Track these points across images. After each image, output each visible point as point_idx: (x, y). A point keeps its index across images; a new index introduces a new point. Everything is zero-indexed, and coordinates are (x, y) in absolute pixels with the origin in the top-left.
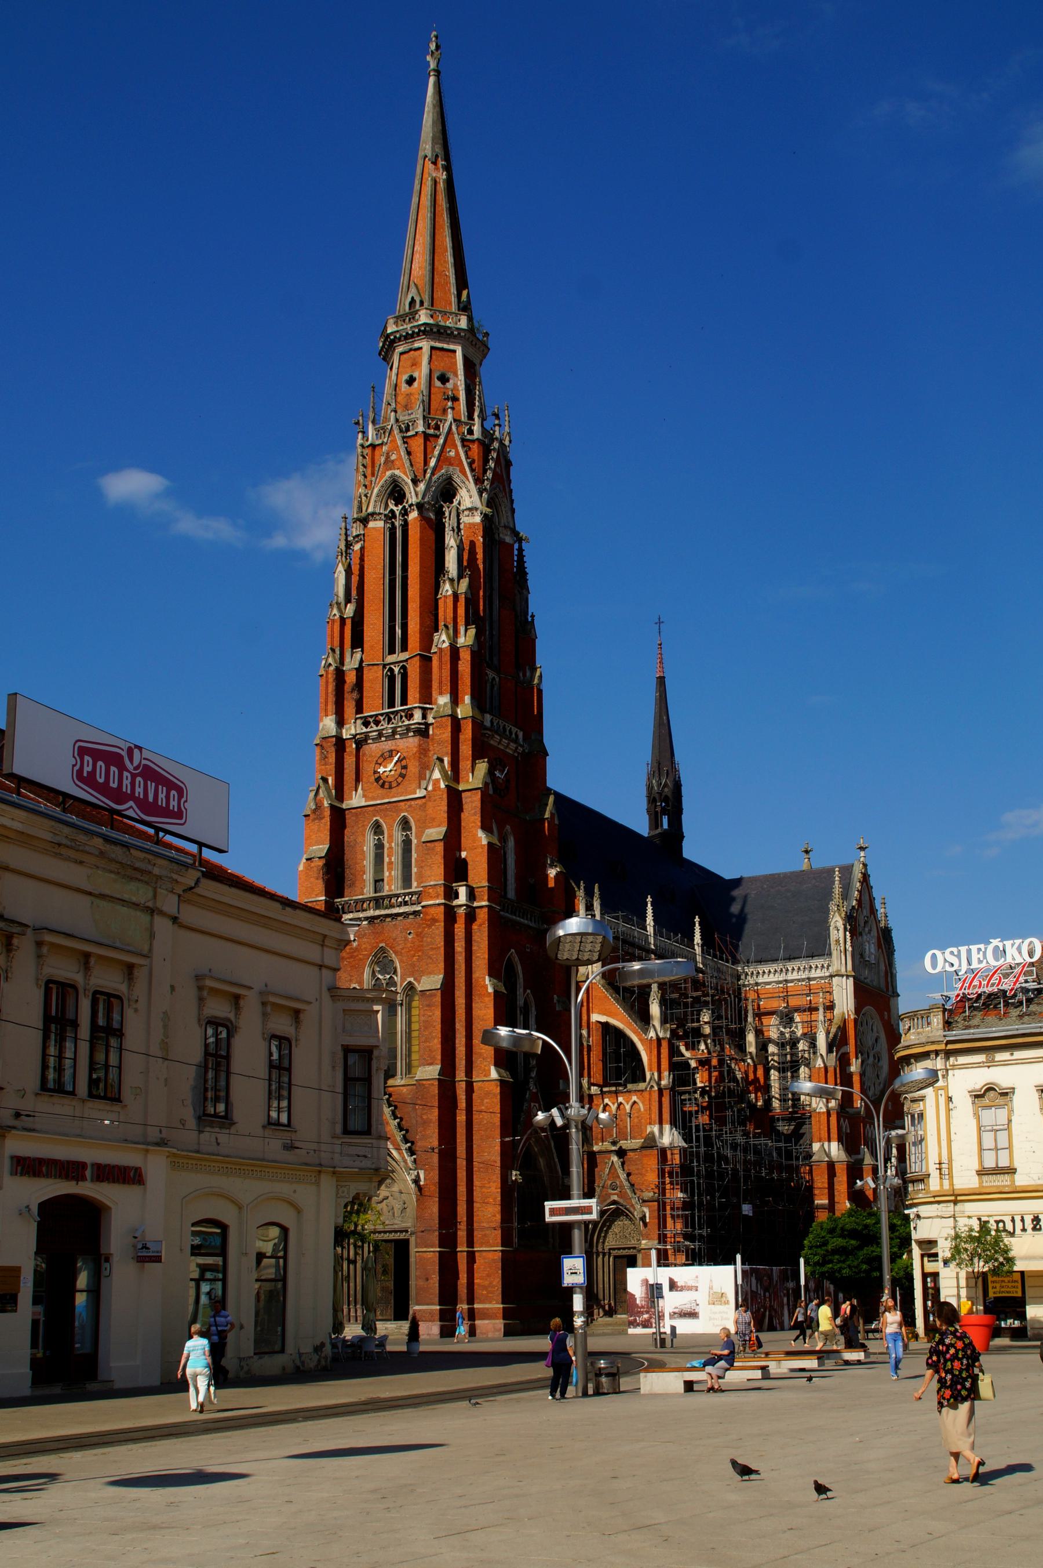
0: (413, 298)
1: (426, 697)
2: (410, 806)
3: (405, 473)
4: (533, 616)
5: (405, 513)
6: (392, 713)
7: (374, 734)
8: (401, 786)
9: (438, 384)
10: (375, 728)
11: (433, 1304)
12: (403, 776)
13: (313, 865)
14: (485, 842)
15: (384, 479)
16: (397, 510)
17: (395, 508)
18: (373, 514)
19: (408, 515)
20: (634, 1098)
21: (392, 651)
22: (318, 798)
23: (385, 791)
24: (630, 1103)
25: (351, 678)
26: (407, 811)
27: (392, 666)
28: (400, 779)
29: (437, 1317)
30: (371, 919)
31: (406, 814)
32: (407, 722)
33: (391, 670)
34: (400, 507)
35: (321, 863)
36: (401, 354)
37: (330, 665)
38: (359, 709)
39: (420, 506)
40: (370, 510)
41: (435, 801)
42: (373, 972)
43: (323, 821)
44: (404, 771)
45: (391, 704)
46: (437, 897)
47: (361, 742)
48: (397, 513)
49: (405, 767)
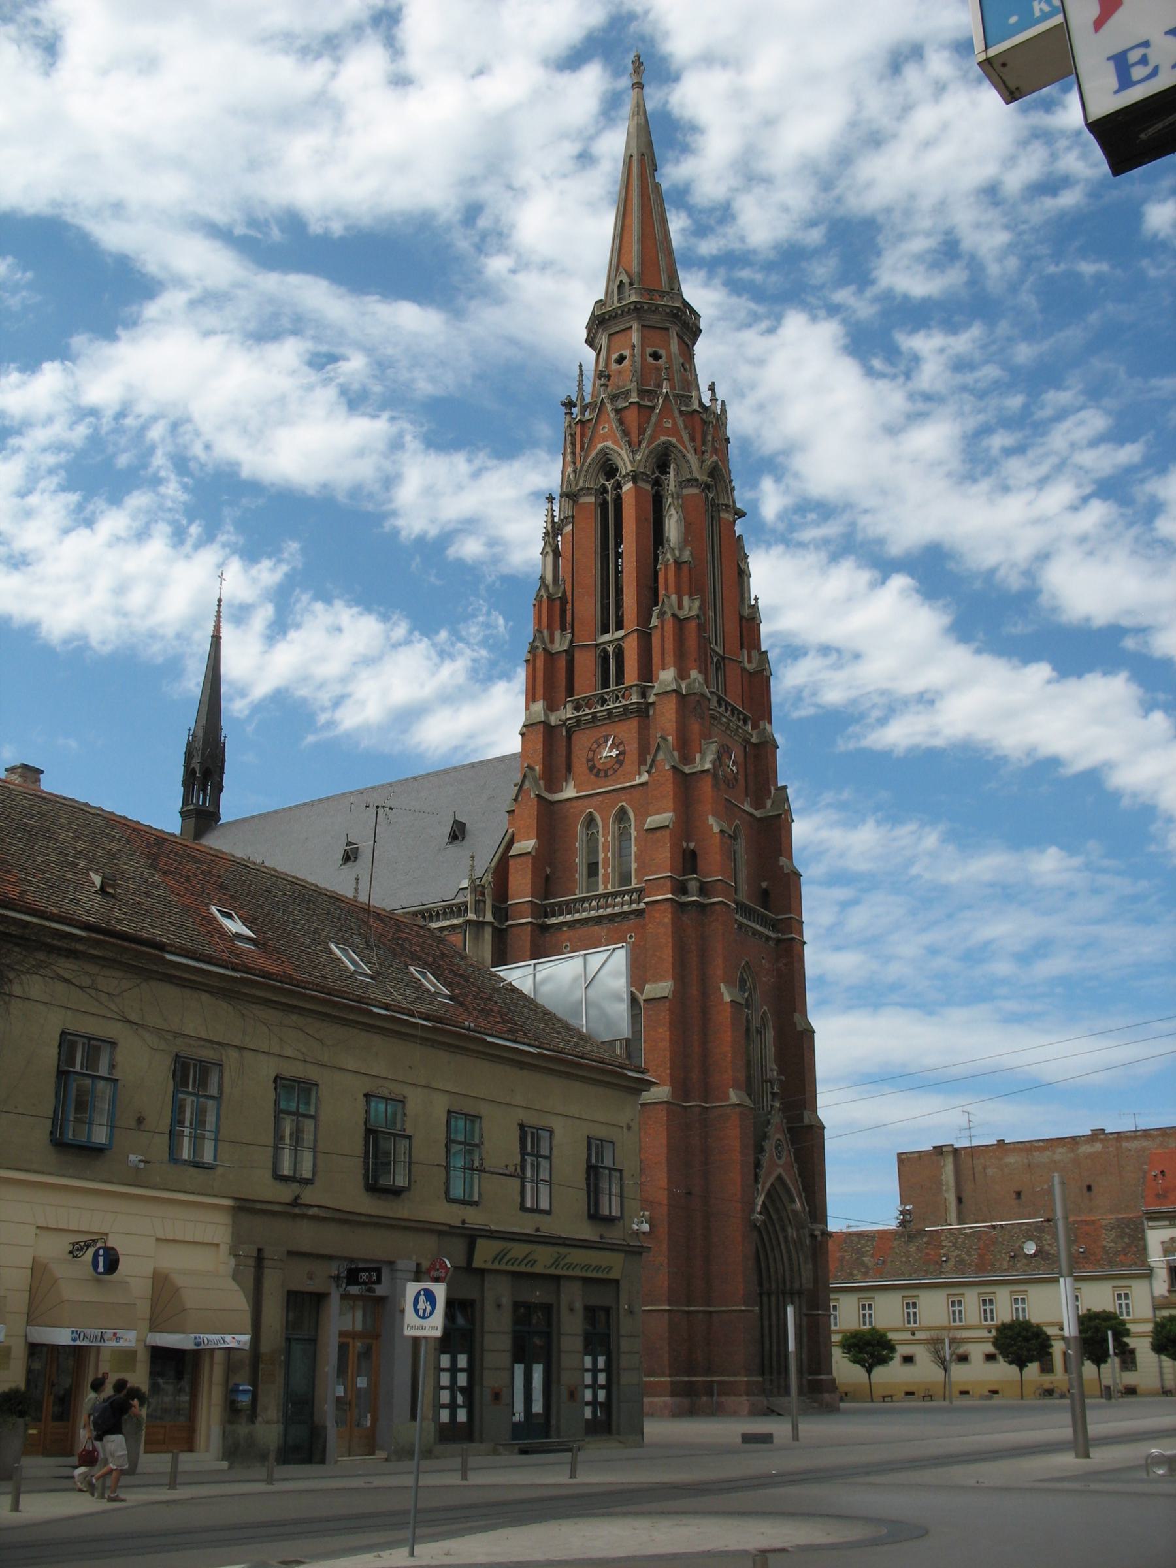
0: (621, 281)
1: (647, 673)
4: (756, 599)
5: (618, 486)
6: (607, 693)
9: (650, 360)
10: (588, 711)
11: (663, 1375)
14: (716, 829)
16: (609, 484)
17: (606, 483)
18: (582, 489)
19: (621, 489)
21: (605, 630)
27: (606, 646)
28: (616, 766)
31: (624, 804)
32: (624, 702)
33: (605, 651)
34: (612, 481)
38: (570, 691)
39: (635, 478)
40: (581, 484)
45: (606, 684)
48: (609, 487)
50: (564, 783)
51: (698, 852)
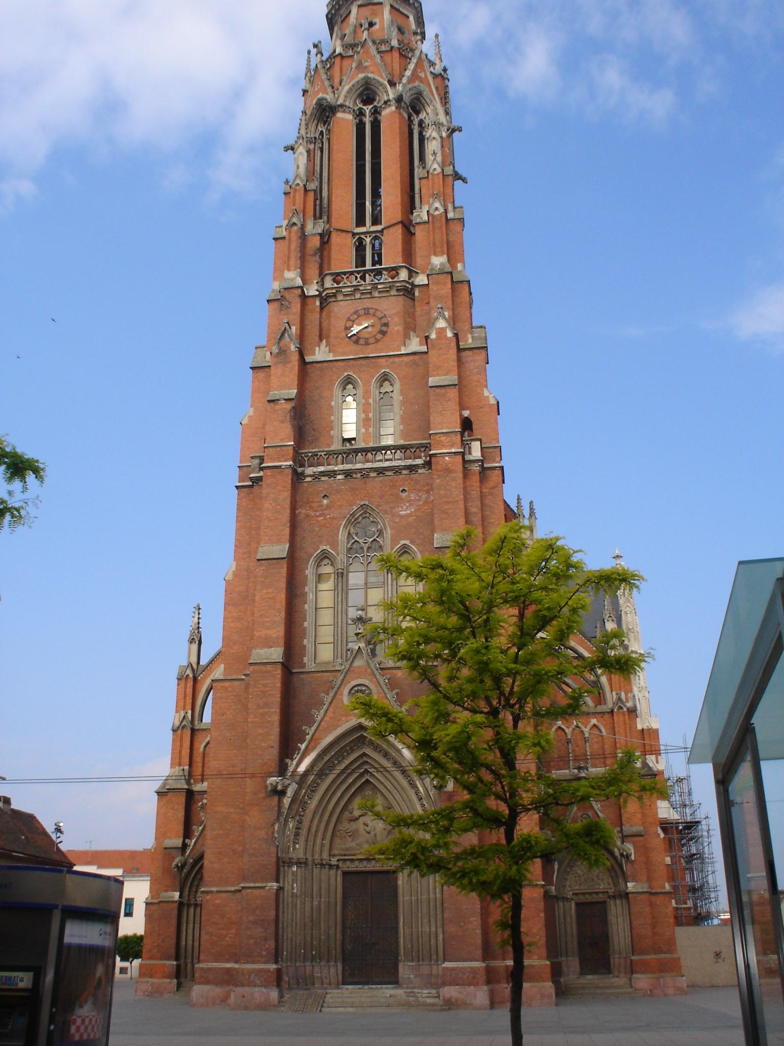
2: (393, 363)
3: (381, 76)
7: (349, 290)
8: (380, 343)
12: (384, 333)
13: (277, 407)
15: (356, 80)
16: (367, 109)
18: (341, 106)
19: (380, 114)
20: (594, 721)
22: (283, 342)
23: (359, 347)
24: (589, 727)
25: (315, 242)
26: (388, 367)
27: (363, 236)
28: (379, 336)
29: (482, 978)
30: (348, 474)
33: (360, 241)
35: (289, 406)
36: (359, 6)
37: (294, 224)
41: (440, 349)
42: (349, 533)
43: (289, 365)
44: (384, 329)
46: (452, 446)
47: (325, 300)
49: (386, 325)
50: (317, 348)
51: (472, 419)
